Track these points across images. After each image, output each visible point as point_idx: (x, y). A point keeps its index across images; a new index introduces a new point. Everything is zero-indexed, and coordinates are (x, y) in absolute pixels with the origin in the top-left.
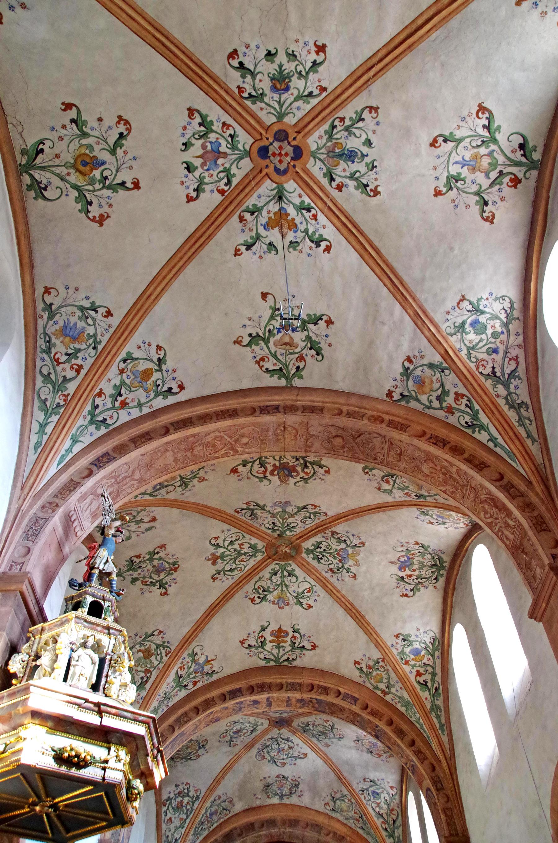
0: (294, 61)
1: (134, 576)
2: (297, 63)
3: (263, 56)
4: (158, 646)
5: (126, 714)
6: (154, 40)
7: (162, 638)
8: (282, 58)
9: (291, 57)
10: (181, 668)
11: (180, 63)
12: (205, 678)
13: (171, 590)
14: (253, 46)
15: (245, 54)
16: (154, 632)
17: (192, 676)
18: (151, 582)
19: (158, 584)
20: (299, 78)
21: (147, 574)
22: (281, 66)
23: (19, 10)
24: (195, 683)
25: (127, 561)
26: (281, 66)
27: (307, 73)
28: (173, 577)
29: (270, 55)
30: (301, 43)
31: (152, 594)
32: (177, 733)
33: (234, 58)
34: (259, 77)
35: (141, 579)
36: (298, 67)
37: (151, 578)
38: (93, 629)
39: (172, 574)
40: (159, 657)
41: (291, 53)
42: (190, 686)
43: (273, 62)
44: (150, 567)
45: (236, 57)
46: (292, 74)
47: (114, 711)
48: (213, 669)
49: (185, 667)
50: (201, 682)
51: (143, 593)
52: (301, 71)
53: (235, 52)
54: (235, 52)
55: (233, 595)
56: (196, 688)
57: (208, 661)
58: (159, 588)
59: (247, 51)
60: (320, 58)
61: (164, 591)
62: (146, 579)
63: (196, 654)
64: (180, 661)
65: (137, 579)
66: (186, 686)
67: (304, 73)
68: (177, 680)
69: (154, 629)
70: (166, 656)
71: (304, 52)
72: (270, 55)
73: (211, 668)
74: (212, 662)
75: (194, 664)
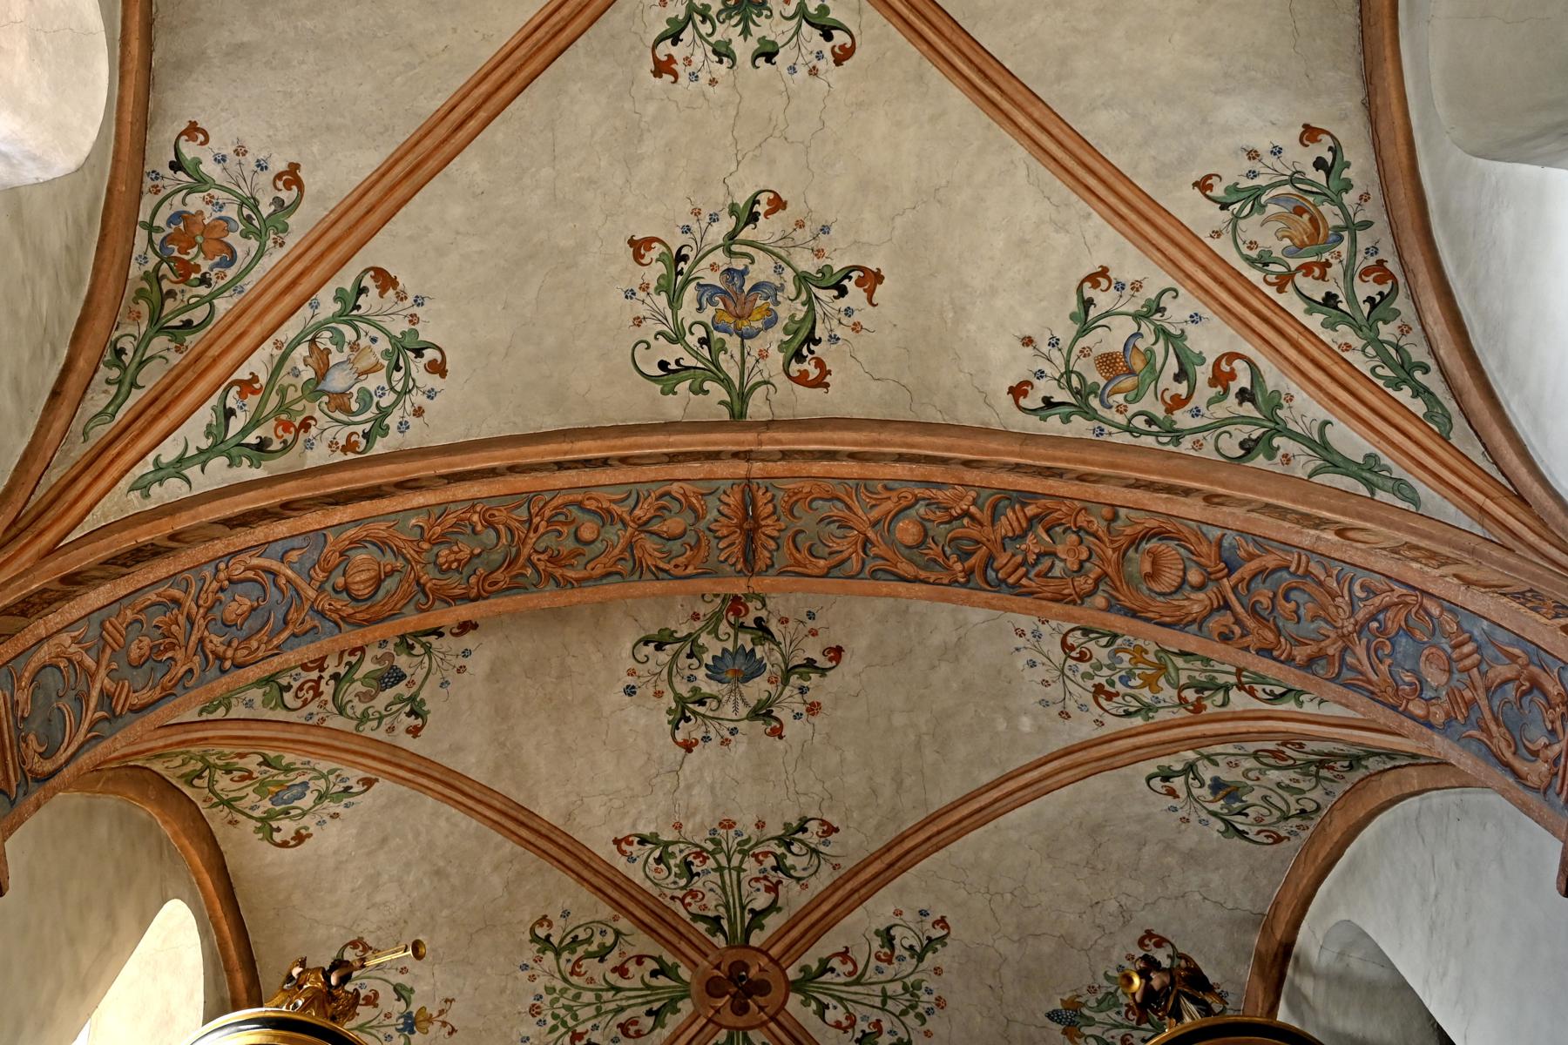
0: (719, 41)
2: (712, 40)
3: (781, 51)
6: (1004, 86)
8: (743, 49)
9: (723, 50)
11: (954, 38)
14: (802, 71)
15: (820, 56)
20: (707, 7)
22: (746, 32)
23: (1263, 146)
26: (746, 32)
27: (689, 18)
29: (768, 53)
30: (704, 78)
33: (842, 47)
34: (791, 9)
36: (710, 31)
41: (725, 59)
43: (762, 40)
45: (837, 50)
46: (722, 17)
52: (703, 22)
53: (838, 61)
54: (838, 61)
59: (815, 61)
60: (665, 48)
67: (698, 18)
71: (698, 58)
72: (768, 53)
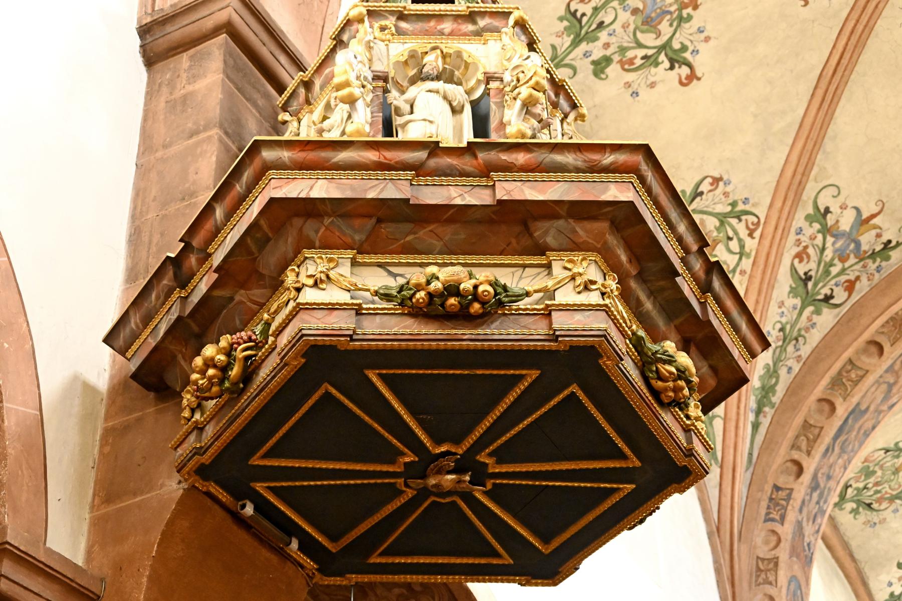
1: (597, 54)
4: (722, 219)
5: (559, 158)
7: (726, 194)
10: (799, 256)
12: (872, 266)
13: (701, 63)
16: (698, 185)
17: (834, 270)
18: (645, 57)
19: (662, 57)
21: (627, 41)
24: (850, 287)
25: (561, 19)
28: (695, 24)
31: (658, 88)
32: (842, 410)
35: (616, 58)
37: (640, 45)
38: (427, 33)
39: (689, 18)
40: (734, 245)
42: (840, 296)
44: (625, 16)
47: (521, 158)
48: (885, 239)
49: (811, 251)
50: (864, 279)
51: (635, 94)
55: (869, 27)
56: (855, 297)
57: (863, 222)
58: (672, 68)
61: (685, 71)
62: (630, 54)
63: (827, 210)
64: (792, 238)
65: (607, 60)
66: (828, 298)
68: (801, 289)
69: (697, 179)
70: (751, 235)
73: (879, 236)
74: (875, 221)
75: (830, 240)
